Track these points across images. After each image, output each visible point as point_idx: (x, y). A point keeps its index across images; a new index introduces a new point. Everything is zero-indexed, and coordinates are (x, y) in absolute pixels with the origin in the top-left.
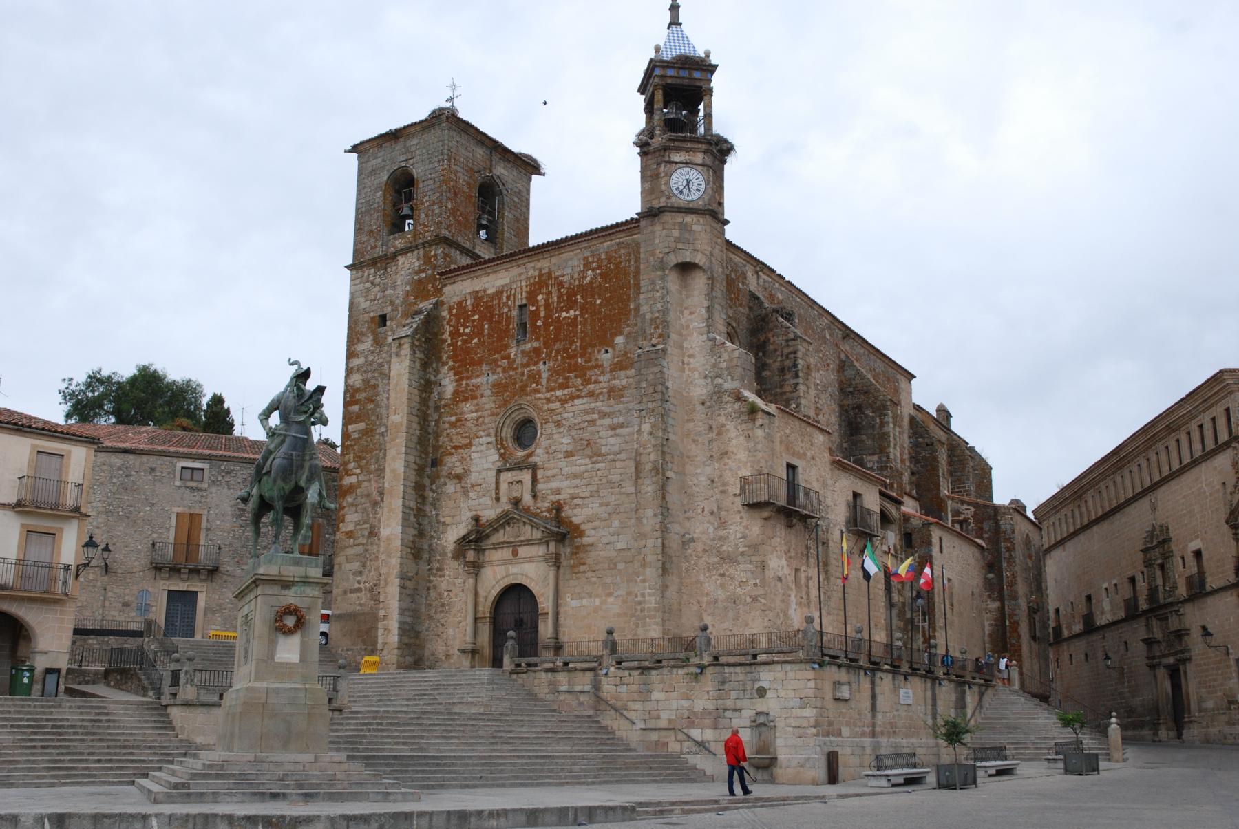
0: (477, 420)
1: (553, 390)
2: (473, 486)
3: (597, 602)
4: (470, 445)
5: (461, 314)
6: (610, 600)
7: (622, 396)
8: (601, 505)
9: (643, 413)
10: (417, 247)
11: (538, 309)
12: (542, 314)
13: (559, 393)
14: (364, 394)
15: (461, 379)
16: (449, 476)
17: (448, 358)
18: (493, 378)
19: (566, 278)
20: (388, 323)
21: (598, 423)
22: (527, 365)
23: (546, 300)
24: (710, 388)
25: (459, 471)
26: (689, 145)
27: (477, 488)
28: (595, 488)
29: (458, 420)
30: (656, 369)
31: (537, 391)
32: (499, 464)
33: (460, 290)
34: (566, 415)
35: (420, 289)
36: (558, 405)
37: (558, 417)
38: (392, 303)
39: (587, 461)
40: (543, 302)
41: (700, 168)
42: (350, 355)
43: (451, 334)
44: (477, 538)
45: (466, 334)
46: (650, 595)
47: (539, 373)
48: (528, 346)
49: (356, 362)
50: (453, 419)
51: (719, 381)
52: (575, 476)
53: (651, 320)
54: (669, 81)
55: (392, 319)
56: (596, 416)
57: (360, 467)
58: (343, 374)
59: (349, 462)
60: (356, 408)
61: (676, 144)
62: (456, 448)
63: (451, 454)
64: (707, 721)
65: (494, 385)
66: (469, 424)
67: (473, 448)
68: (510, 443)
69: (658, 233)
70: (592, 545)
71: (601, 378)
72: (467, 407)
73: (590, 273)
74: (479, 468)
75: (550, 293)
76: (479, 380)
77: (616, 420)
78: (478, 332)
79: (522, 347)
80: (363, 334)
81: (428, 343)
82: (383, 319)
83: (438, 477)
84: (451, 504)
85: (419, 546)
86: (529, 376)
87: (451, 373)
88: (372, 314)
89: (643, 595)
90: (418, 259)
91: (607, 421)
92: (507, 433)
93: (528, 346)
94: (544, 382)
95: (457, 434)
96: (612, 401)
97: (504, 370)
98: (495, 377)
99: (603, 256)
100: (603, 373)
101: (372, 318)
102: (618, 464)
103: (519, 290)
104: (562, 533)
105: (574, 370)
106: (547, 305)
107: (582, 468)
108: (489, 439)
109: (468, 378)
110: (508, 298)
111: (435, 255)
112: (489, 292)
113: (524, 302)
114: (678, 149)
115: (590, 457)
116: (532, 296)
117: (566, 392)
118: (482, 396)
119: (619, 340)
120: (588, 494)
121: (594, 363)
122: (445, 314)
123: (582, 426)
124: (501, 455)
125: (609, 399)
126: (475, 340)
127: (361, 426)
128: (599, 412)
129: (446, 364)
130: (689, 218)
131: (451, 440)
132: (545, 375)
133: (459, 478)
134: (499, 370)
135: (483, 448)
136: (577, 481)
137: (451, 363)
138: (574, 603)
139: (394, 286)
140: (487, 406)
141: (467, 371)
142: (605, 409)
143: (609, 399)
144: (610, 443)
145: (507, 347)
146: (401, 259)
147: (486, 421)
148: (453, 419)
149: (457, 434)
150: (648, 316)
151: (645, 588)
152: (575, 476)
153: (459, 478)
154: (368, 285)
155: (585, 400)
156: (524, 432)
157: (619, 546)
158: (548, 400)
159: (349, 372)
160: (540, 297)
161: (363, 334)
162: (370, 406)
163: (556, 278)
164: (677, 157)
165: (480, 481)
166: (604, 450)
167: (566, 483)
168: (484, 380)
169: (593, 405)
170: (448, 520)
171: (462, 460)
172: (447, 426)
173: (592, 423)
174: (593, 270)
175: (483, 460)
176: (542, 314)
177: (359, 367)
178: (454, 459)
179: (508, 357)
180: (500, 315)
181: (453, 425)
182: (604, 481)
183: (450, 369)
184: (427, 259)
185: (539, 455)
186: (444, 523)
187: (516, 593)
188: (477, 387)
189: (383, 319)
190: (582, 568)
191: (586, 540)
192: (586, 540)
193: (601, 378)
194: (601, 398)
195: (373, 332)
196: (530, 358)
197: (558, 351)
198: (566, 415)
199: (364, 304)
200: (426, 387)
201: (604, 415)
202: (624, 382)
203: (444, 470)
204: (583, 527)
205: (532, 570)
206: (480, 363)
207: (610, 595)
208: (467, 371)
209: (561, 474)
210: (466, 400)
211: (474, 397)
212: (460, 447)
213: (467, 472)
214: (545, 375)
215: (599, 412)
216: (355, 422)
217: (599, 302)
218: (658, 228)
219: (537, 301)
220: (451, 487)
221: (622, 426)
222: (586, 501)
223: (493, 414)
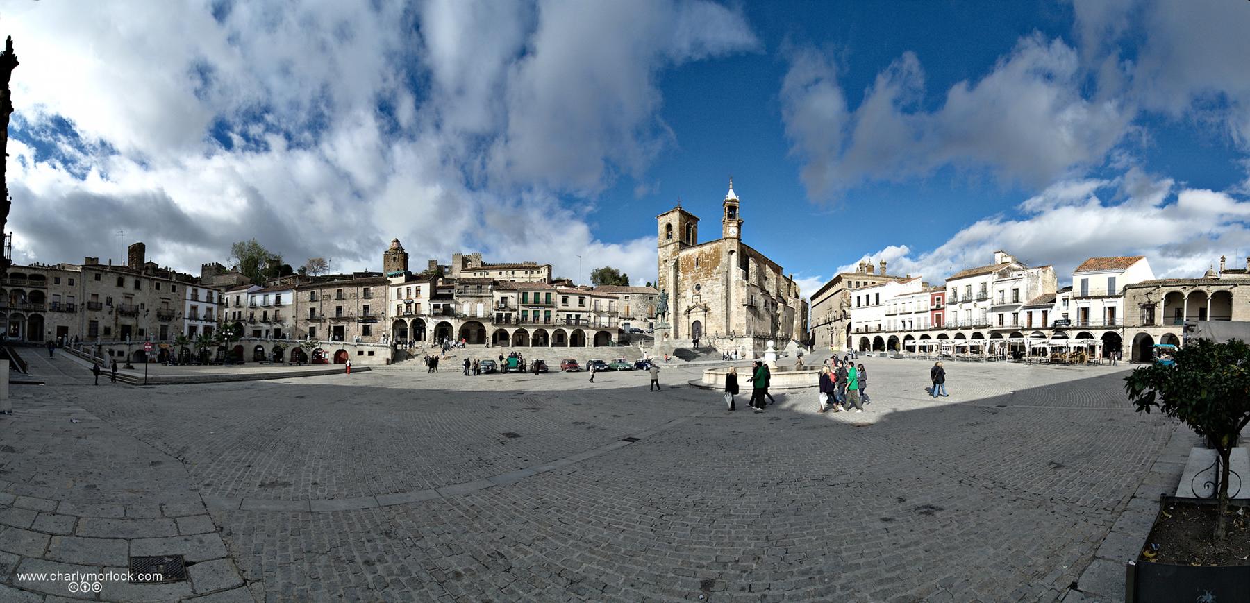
5: (684, 260)
33: (683, 254)
35: (674, 254)
44: (689, 311)
81: (676, 266)
85: (676, 313)
104: (706, 310)
105: (708, 274)
144: (716, 290)
156: (698, 288)
168: (689, 276)
175: (689, 293)
185: (701, 292)
187: (697, 322)
200: (677, 277)
205: (700, 316)
209: (706, 297)
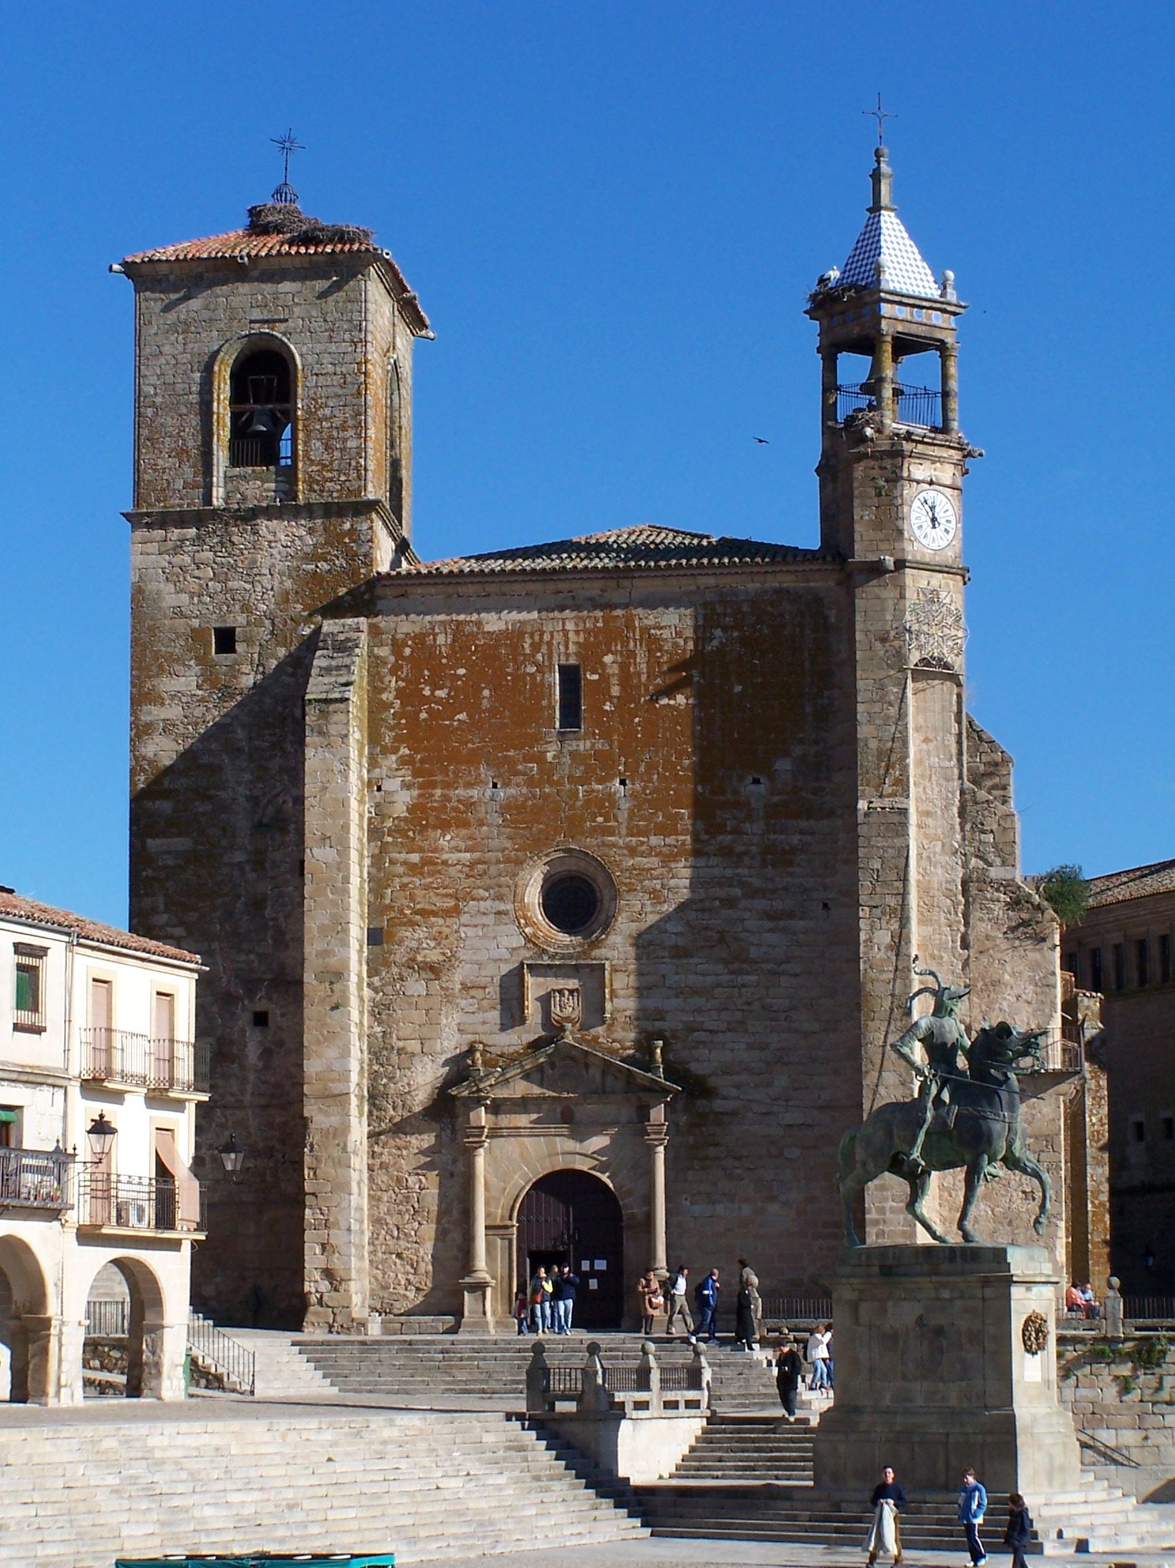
0: (472, 865)
1: (639, 834)
2: (465, 987)
3: (746, 1209)
4: (455, 911)
6: (774, 1208)
7: (791, 863)
8: (750, 1047)
9: (878, 912)
10: (309, 511)
11: (605, 678)
12: (615, 691)
13: (654, 840)
14: (185, 782)
15: (433, 785)
16: (411, 964)
17: (399, 739)
18: (501, 793)
19: (666, 634)
20: (240, 647)
21: (743, 904)
22: (584, 781)
23: (624, 667)
24: (960, 873)
25: (434, 956)
26: (937, 452)
27: (479, 993)
28: (739, 1015)
29: (425, 862)
30: (898, 842)
31: (610, 832)
32: (526, 955)
34: (673, 882)
36: (654, 861)
37: (657, 884)
38: (246, 608)
39: (720, 968)
40: (615, 669)
41: (948, 492)
42: (141, 697)
43: (400, 694)
45: (439, 701)
46: (892, 1210)
47: (611, 797)
48: (583, 746)
49: (153, 713)
50: (415, 858)
51: (974, 862)
52: (695, 992)
53: (880, 752)
54: (900, 329)
55: (249, 641)
56: (737, 892)
57: (181, 923)
58: (126, 734)
59: (154, 911)
60: (165, 806)
61: (920, 448)
62: (423, 913)
63: (412, 924)
64: (1125, 1419)
65: (506, 807)
66: (452, 871)
67: (465, 918)
68: (539, 916)
69: (890, 603)
70: (734, 1114)
71: (747, 827)
72: (446, 840)
73: (718, 632)
74: (483, 956)
75: (632, 654)
76: (474, 793)
77: (778, 905)
78: (465, 697)
79: (572, 745)
80: (177, 660)
82: (226, 640)
83: (387, 964)
84: (419, 1016)
86: (588, 803)
87: (406, 773)
88: (195, 623)
89: (881, 1211)
90: (311, 531)
91: (761, 904)
92: (533, 895)
93: (583, 746)
94: (623, 816)
95: (427, 887)
96: (769, 870)
97: (531, 782)
98: (512, 791)
99: (745, 608)
100: (750, 818)
101: (197, 635)
102: (784, 981)
103: (558, 638)
106: (626, 678)
107: (710, 980)
108: (502, 907)
109: (447, 785)
110: (536, 647)
111: (352, 530)
112: (487, 628)
113: (572, 661)
114: (922, 456)
115: (726, 962)
116: (591, 652)
117: (670, 840)
118: (481, 823)
119: (783, 765)
120: (723, 1026)
121: (730, 796)
122: (384, 652)
123: (707, 904)
124: (528, 939)
125: (764, 864)
126: (462, 716)
127: (182, 843)
128: (743, 885)
129: (395, 750)
130: (937, 579)
131: (412, 898)
132: (625, 805)
133: (434, 970)
134: (520, 779)
135: (489, 920)
136: (699, 1001)
137: (404, 751)
138: (697, 1210)
139: (252, 576)
140: (494, 843)
141: (445, 771)
142: (756, 882)
143: (764, 864)
145: (537, 739)
146: (264, 525)
147: (493, 870)
148: (415, 858)
149: (427, 887)
150: (873, 744)
151: (885, 1199)
152: (695, 992)
153: (434, 970)
154: (177, 560)
155: (714, 861)
157: (789, 1118)
158: (633, 851)
159: (140, 731)
160: (608, 659)
161: (172, 659)
162: (203, 807)
163: (645, 630)
164: (919, 471)
165: (483, 981)
166: (753, 952)
167: (675, 1002)
168: (485, 793)
169: (729, 872)
170: (414, 1046)
171: (439, 938)
172: (400, 869)
173: (730, 902)
174: (725, 629)
176: (615, 691)
177: (168, 727)
178: (421, 933)
179: (540, 759)
180: (519, 678)
181: (413, 869)
182: (756, 1006)
183: (403, 761)
184: (334, 539)
186: (400, 1051)
188: (470, 805)
189: (226, 640)
190: (712, 1152)
191: (718, 1105)
192: (718, 1105)
193: (747, 827)
194: (747, 860)
195: (200, 660)
196: (589, 770)
197: (651, 767)
198: (673, 882)
199: (171, 598)
201: (755, 893)
202: (796, 839)
203: (400, 955)
204: (712, 1082)
206: (473, 759)
207: (772, 1199)
208: (445, 771)
210: (445, 826)
211: (465, 824)
212: (434, 914)
213: (451, 959)
214: (625, 805)
215: (743, 885)
216: (161, 834)
217: (738, 689)
218: (890, 594)
219: (603, 665)
220: (416, 986)
221: (791, 915)
222: (720, 1038)
223: (508, 860)
